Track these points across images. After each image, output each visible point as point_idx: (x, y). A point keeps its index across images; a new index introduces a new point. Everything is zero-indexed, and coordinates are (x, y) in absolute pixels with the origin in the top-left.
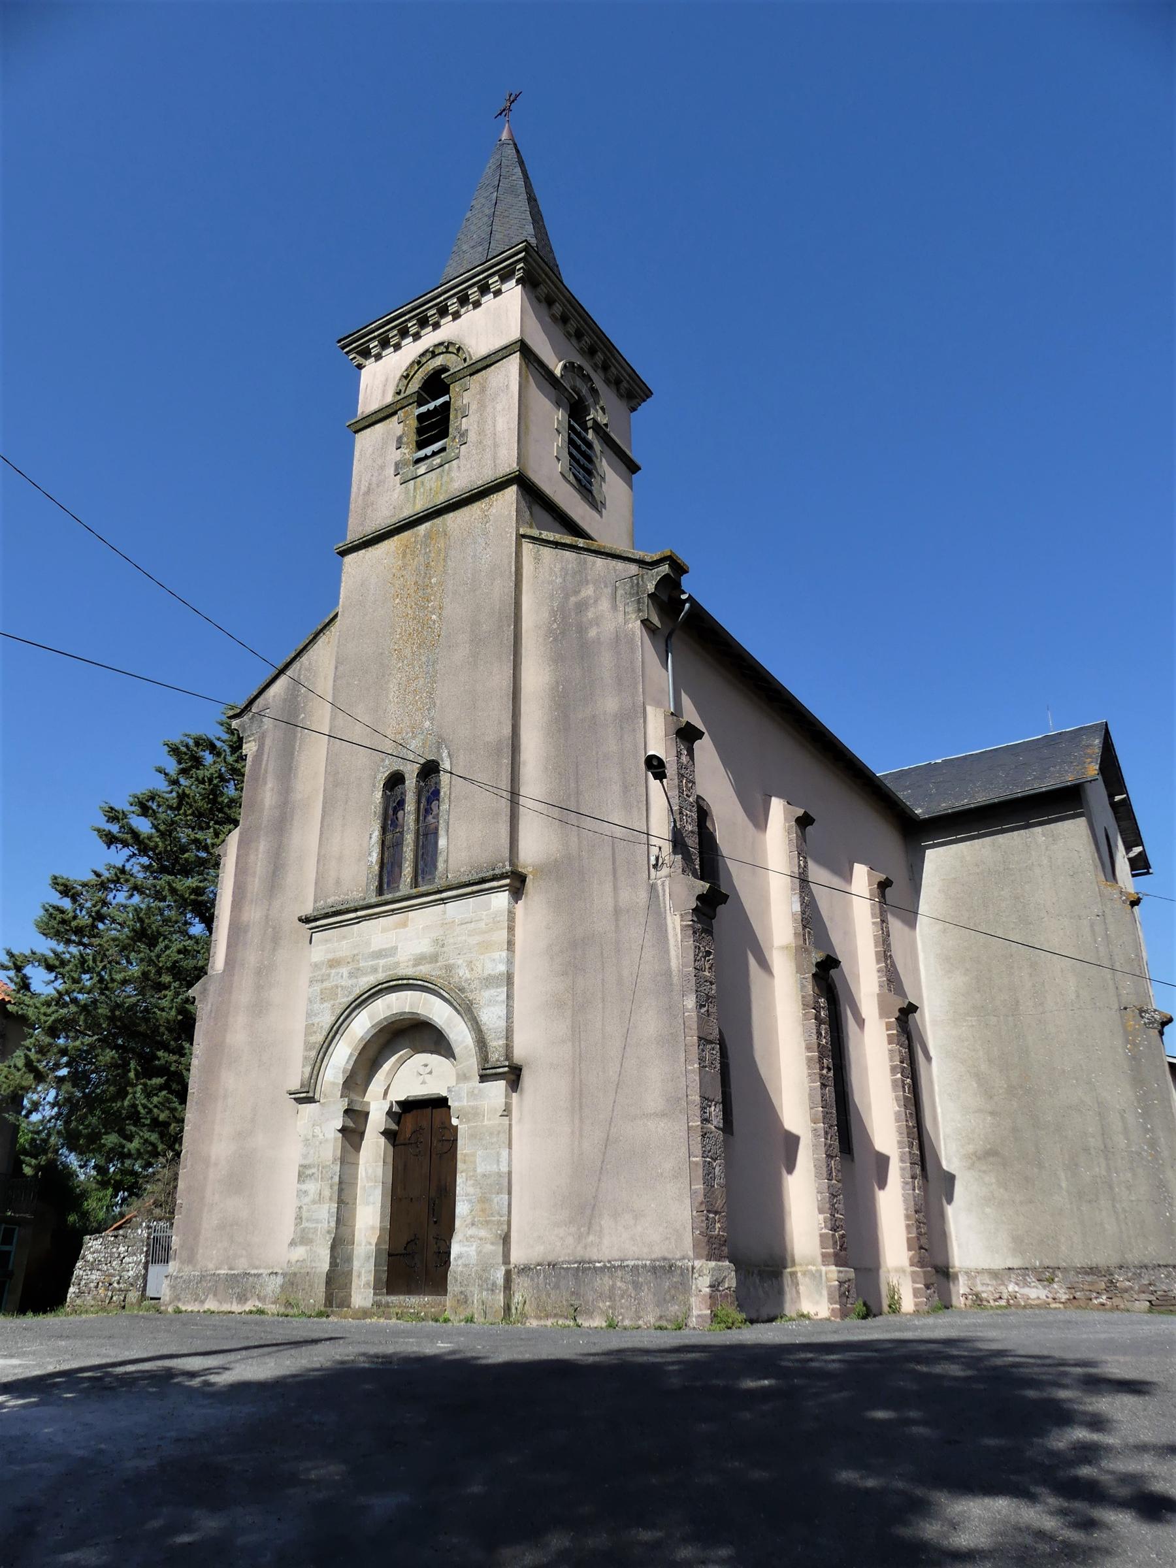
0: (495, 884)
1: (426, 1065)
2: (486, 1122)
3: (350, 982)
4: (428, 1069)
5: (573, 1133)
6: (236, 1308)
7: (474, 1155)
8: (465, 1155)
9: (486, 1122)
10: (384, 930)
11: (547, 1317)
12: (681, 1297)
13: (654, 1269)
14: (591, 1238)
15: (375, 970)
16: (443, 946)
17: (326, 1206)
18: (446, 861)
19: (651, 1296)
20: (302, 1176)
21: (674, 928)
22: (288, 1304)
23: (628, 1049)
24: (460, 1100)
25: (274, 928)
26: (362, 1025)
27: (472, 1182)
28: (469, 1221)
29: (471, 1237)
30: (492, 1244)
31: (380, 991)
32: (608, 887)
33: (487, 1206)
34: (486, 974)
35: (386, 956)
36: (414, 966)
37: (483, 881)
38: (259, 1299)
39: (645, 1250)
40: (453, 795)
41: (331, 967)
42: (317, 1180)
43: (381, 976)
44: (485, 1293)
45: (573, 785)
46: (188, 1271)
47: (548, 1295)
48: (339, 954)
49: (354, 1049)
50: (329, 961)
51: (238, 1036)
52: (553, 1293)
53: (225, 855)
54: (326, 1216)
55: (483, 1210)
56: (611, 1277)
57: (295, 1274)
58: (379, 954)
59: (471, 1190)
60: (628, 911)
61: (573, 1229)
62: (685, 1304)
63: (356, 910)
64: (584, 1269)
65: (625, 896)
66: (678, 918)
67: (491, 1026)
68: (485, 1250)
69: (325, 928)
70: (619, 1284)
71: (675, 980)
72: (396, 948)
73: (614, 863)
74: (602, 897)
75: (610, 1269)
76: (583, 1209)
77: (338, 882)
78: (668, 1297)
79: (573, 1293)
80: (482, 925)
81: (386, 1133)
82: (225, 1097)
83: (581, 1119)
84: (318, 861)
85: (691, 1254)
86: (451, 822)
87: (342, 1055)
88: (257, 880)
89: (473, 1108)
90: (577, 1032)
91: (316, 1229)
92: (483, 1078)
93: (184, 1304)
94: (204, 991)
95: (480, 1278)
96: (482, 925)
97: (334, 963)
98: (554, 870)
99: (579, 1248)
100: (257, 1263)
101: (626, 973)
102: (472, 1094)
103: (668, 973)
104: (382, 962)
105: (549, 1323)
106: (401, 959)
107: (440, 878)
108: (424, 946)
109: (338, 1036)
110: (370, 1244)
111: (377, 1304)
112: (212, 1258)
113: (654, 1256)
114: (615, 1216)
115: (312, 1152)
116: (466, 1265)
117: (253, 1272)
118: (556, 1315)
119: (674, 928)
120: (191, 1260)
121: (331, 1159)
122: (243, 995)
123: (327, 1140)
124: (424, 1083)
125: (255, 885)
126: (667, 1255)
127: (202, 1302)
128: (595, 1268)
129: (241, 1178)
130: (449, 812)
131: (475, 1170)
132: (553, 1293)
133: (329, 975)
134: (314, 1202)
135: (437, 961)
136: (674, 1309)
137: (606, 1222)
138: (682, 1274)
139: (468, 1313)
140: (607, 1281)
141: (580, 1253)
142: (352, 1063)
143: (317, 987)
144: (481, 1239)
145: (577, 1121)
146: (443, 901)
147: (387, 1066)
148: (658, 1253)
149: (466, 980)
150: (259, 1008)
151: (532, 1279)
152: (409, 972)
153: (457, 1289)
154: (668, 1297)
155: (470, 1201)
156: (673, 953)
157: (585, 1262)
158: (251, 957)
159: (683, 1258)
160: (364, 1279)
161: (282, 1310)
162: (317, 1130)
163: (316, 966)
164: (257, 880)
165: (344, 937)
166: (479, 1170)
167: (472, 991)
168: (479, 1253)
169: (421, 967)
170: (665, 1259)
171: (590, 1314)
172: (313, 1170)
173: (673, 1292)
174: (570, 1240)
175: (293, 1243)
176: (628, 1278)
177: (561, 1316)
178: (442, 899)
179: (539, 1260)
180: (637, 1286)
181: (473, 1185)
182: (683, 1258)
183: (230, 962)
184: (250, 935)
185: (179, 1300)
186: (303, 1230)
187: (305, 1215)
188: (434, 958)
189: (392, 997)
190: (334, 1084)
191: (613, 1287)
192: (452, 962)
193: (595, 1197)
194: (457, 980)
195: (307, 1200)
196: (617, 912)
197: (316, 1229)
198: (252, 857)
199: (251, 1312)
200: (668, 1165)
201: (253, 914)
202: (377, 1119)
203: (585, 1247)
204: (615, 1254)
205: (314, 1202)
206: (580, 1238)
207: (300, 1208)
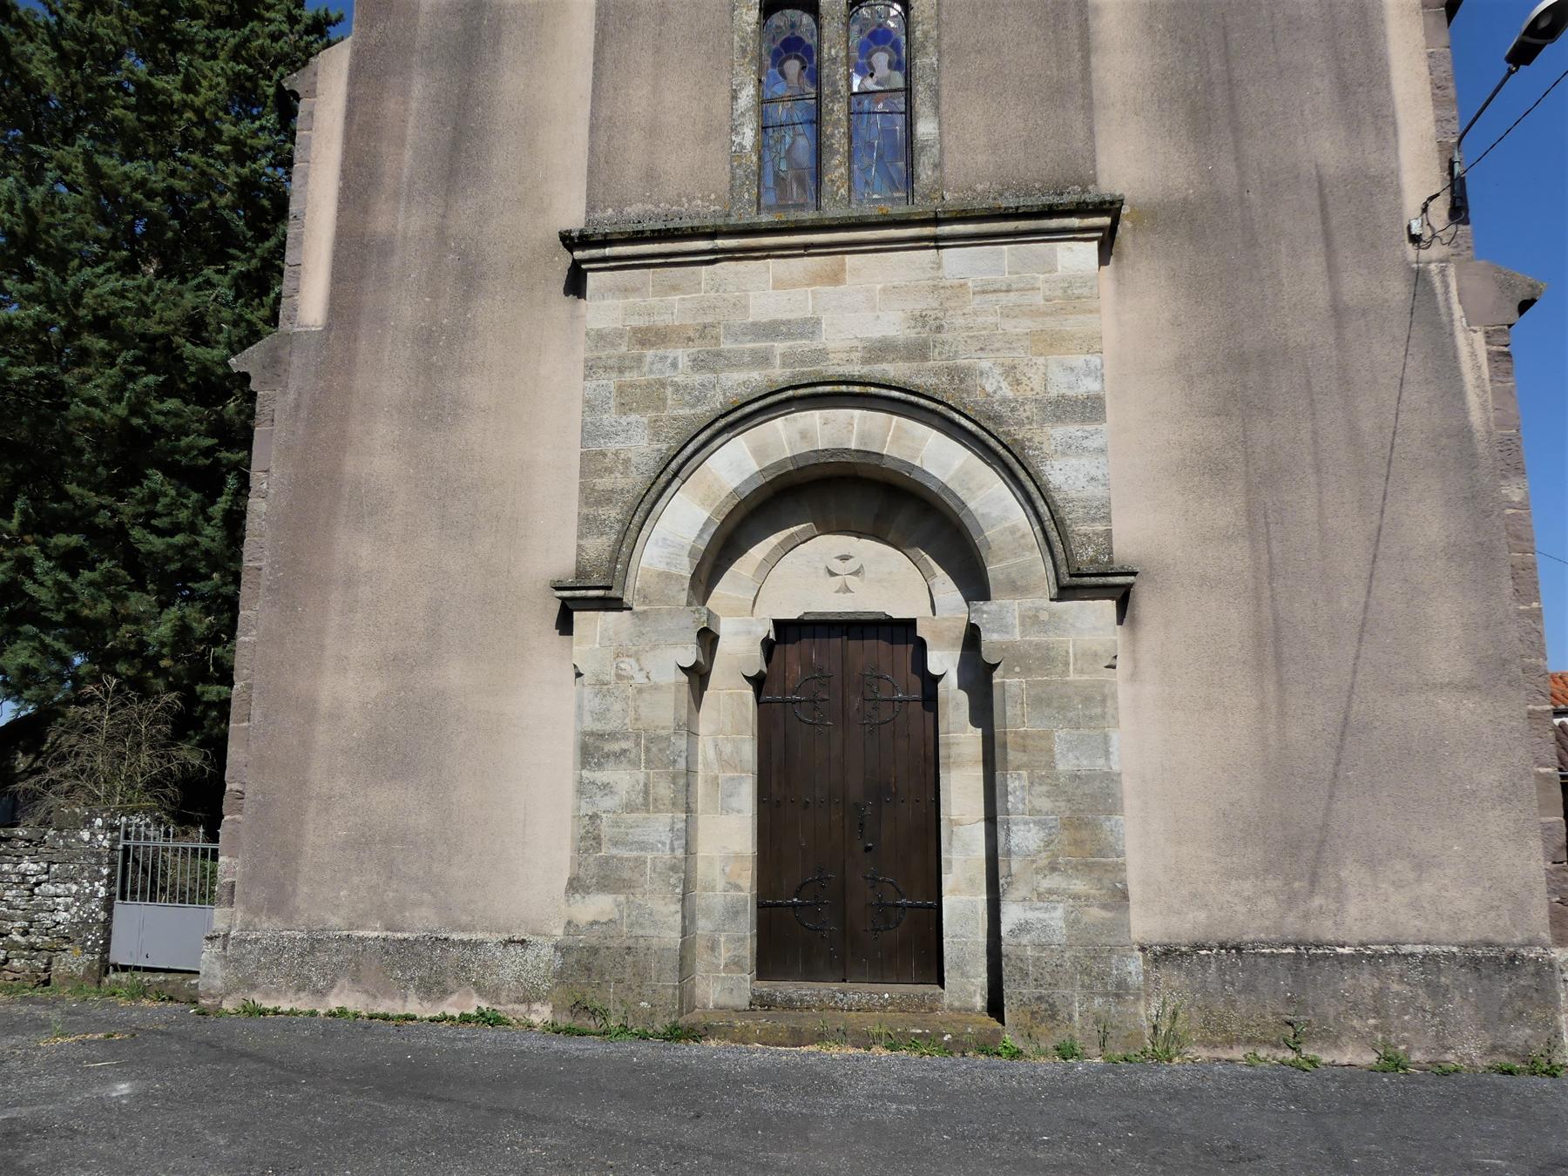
0: (1075, 222)
1: (844, 558)
2: (1072, 677)
3: (698, 378)
4: (852, 565)
5: (1262, 707)
6: (414, 1007)
7: (1047, 736)
8: (1025, 736)
9: (1072, 677)
10: (779, 284)
11: (1230, 1042)
12: (1537, 1014)
13: (1475, 963)
14: (1317, 901)
15: (762, 360)
16: (939, 329)
17: (665, 818)
18: (937, 166)
19: (1468, 1010)
20: (591, 751)
21: (1473, 355)
22: (579, 1008)
23: (1381, 563)
24: (1004, 628)
25: (463, 255)
26: (735, 465)
27: (1044, 788)
28: (1043, 860)
29: (1050, 892)
30: (1104, 907)
31: (789, 401)
32: (1314, 264)
33: (1084, 834)
34: (1053, 393)
35: (789, 336)
36: (866, 361)
37: (1050, 212)
38: (480, 990)
39: (1444, 927)
40: (946, 40)
41: (643, 343)
42: (635, 764)
43: (779, 374)
44: (1098, 1001)
45: (1217, 66)
46: (268, 927)
47: (1232, 1003)
48: (661, 320)
49: (716, 512)
50: (636, 331)
51: (378, 456)
52: (1241, 1000)
53: (312, 93)
54: (666, 837)
55: (1077, 843)
56: (1377, 974)
57: (594, 951)
58: (771, 330)
59: (1044, 804)
60: (1364, 313)
61: (1273, 884)
62: (1546, 1026)
63: (713, 235)
64: (1309, 958)
65: (1354, 285)
66: (1479, 338)
67: (1073, 494)
68: (1085, 919)
69: (623, 263)
70: (1395, 987)
71: (1481, 448)
72: (818, 322)
73: (1325, 220)
74: (1302, 281)
75: (1368, 958)
76: (1297, 847)
77: (651, 176)
78: (1508, 1012)
79: (1290, 1001)
80: (1038, 299)
81: (758, 682)
82: (350, 583)
83: (1280, 683)
84: (593, 129)
85: (1546, 936)
86: (944, 92)
87: (685, 519)
88: (408, 154)
89: (1038, 646)
90: (1259, 523)
91: (639, 863)
92: (1065, 592)
93: (267, 995)
94: (274, 362)
95: (1086, 971)
96: (1038, 299)
97: (648, 337)
98: (1180, 219)
99: (1290, 919)
100: (465, 919)
101: (1367, 425)
102: (1031, 620)
103: (1464, 433)
104: (780, 347)
105: (1238, 1053)
106: (831, 346)
107: (925, 197)
108: (892, 325)
109: (677, 482)
110: (738, 888)
111: (762, 1003)
112: (334, 903)
113: (1463, 938)
114: (1372, 863)
115: (617, 707)
116: (1041, 946)
117: (455, 936)
118: (1250, 1041)
119: (1473, 355)
120: (278, 904)
121: (672, 724)
122: (386, 374)
123: (657, 688)
124: (847, 590)
125: (405, 158)
126: (1491, 936)
127: (321, 993)
128: (1337, 955)
129: (410, 741)
130: (936, 72)
131: (1051, 765)
132: (1241, 1000)
133: (639, 360)
134: (630, 807)
135: (925, 358)
136: (1520, 1035)
137: (1351, 873)
138: (1537, 974)
139: (1060, 1036)
140: (1368, 981)
141: (1292, 925)
142: (707, 538)
143: (610, 381)
144: (1076, 897)
145: (1271, 688)
146: (937, 242)
147: (758, 552)
148: (1472, 931)
149: (1004, 401)
150: (433, 410)
151: (1190, 973)
152: (856, 370)
153: (1029, 991)
154: (1508, 1012)
155: (1041, 824)
156: (1473, 400)
157: (1308, 946)
158: (404, 307)
159: (1530, 944)
160: (724, 955)
161: (564, 1020)
162: (628, 665)
163: (601, 338)
164: (408, 154)
165: (675, 288)
166: (1061, 767)
167: (1020, 423)
168: (1072, 924)
169: (885, 366)
170: (1489, 944)
171: (1333, 1039)
172: (624, 745)
173: (1519, 1004)
174: (1268, 903)
175: (575, 886)
176: (1415, 975)
177: (1263, 1043)
178: (936, 238)
179: (1199, 936)
180: (1435, 990)
181: (1048, 795)
182: (1530, 944)
183: (341, 305)
184: (396, 261)
185: (253, 987)
186: (606, 861)
187: (605, 830)
188: (918, 351)
189: (814, 419)
190: (667, 577)
191: (1379, 995)
192: (961, 362)
193: (1325, 826)
194: (981, 398)
195: (608, 802)
196: (1338, 312)
197: (639, 863)
198: (391, 105)
199: (465, 1019)
200: (1489, 778)
201: (402, 220)
202: (741, 646)
203: (1306, 916)
204: (1375, 930)
205: (630, 807)
206: (1291, 900)
207: (593, 817)
